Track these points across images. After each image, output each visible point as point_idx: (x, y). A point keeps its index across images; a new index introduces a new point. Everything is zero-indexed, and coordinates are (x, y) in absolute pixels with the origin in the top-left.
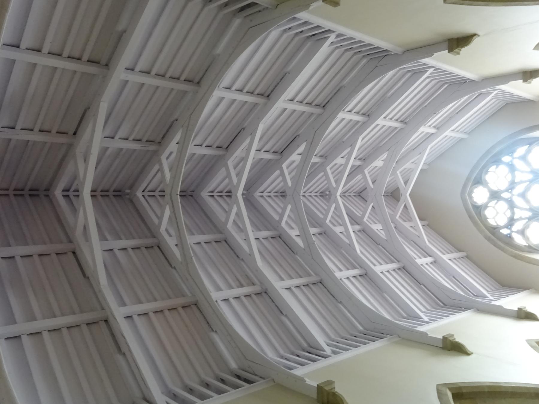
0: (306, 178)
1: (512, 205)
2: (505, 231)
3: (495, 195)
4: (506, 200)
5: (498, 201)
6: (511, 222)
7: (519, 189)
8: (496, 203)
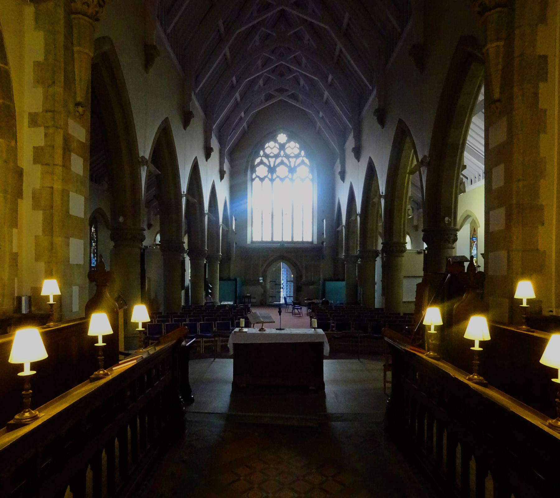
0: (288, 67)
1: (276, 156)
2: (262, 153)
3: (282, 147)
4: (279, 153)
5: (279, 149)
6: (267, 156)
7: (285, 160)
8: (277, 148)
